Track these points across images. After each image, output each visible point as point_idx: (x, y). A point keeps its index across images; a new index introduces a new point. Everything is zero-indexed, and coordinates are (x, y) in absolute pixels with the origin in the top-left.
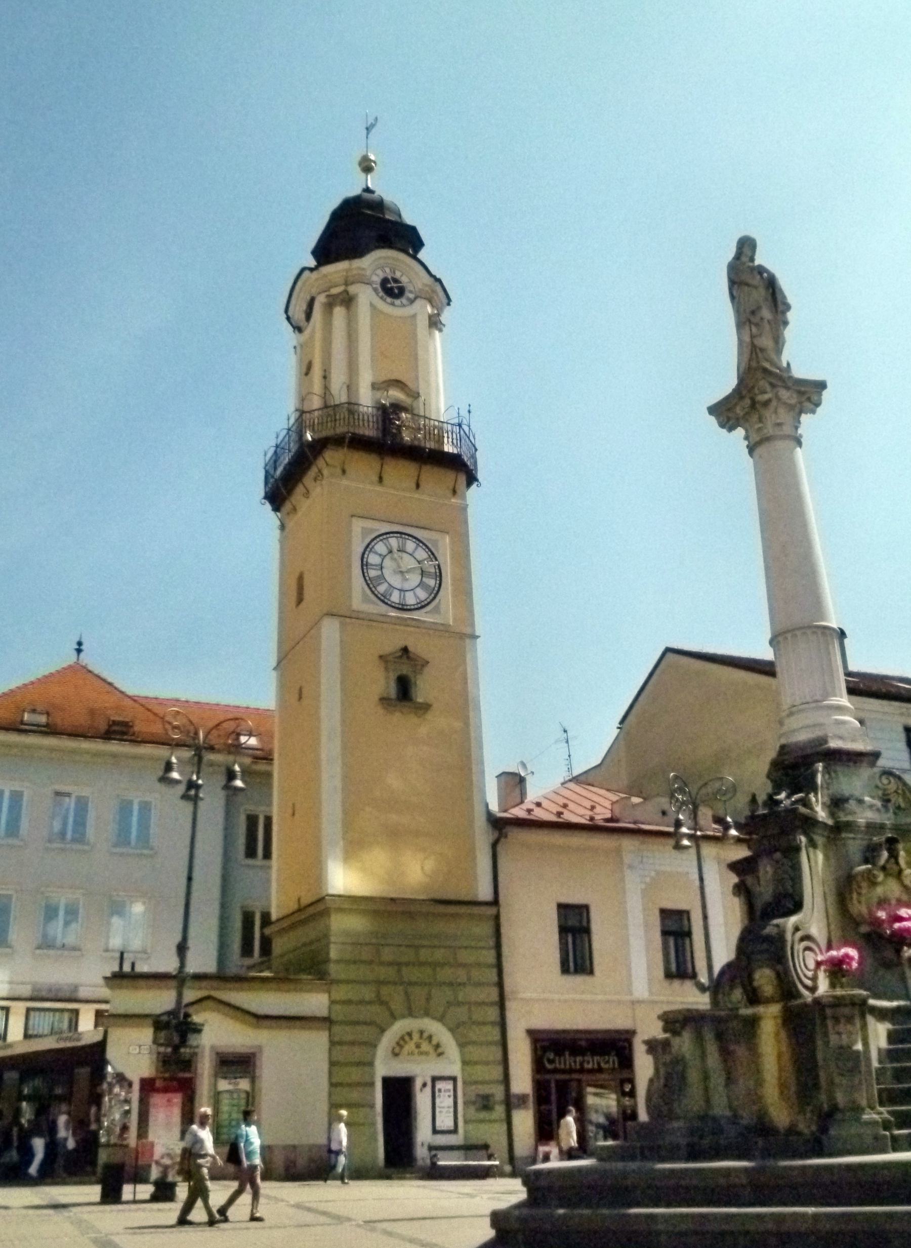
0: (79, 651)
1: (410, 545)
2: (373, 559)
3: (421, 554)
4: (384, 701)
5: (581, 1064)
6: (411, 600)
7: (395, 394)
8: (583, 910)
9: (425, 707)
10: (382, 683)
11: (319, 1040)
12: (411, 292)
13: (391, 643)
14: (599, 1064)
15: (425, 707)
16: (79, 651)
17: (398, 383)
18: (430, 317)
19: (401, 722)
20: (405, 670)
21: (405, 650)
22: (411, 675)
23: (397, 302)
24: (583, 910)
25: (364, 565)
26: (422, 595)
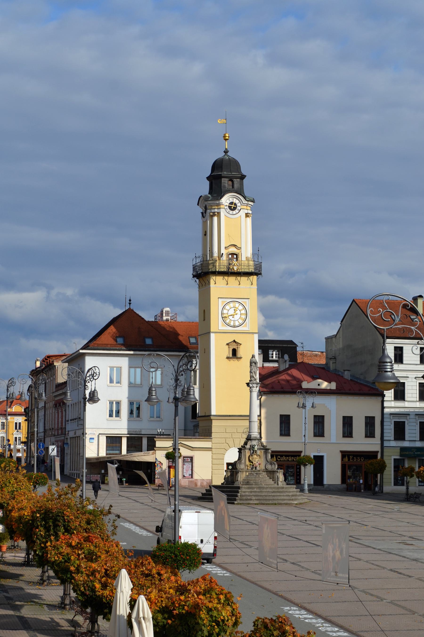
0: (130, 304)
1: (237, 305)
2: (225, 311)
3: (241, 307)
4: (228, 358)
5: (288, 459)
6: (237, 324)
7: (233, 250)
8: (288, 417)
9: (241, 358)
10: (227, 352)
11: (209, 454)
12: (239, 206)
13: (230, 338)
14: (293, 459)
15: (241, 358)
16: (130, 304)
17: (235, 246)
18: (246, 214)
19: (234, 362)
20: (235, 347)
21: (234, 341)
22: (237, 349)
23: (234, 212)
24: (288, 417)
25: (222, 314)
26: (241, 321)
